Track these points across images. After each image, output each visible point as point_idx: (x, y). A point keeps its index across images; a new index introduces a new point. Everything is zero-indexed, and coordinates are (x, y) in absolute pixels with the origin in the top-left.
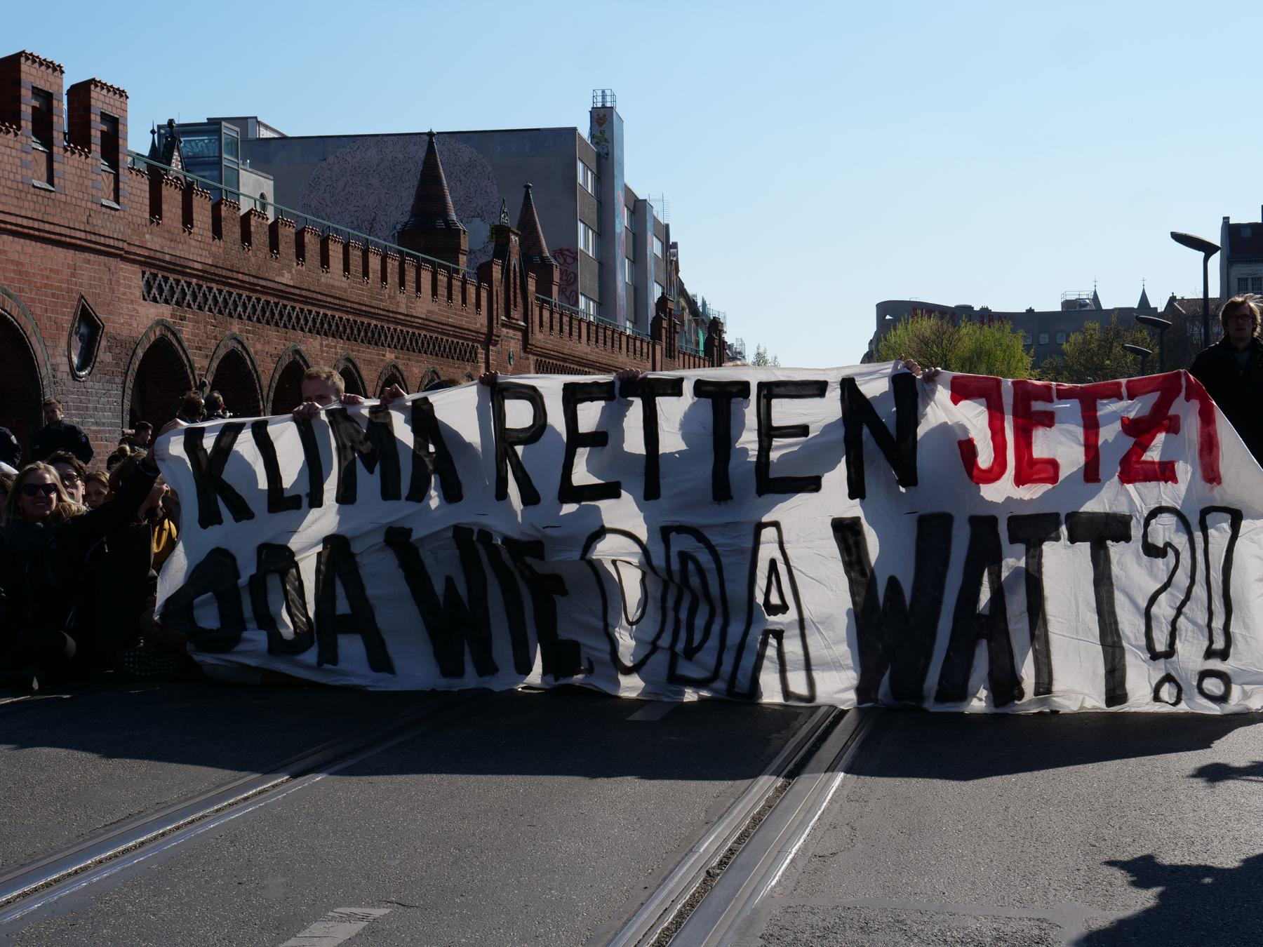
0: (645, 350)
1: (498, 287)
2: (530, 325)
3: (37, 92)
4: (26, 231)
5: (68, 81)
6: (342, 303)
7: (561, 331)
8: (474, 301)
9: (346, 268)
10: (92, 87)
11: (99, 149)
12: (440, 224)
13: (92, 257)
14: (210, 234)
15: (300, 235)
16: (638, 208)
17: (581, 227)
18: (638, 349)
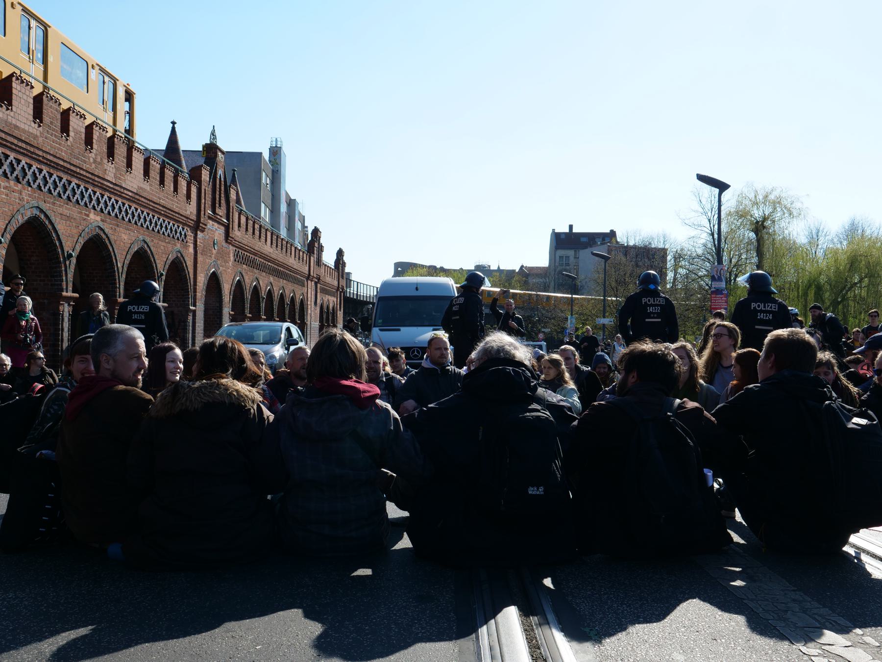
0: (305, 259)
1: (206, 187)
2: (231, 223)
8: (185, 192)
16: (291, 204)
17: (263, 205)
18: (301, 257)
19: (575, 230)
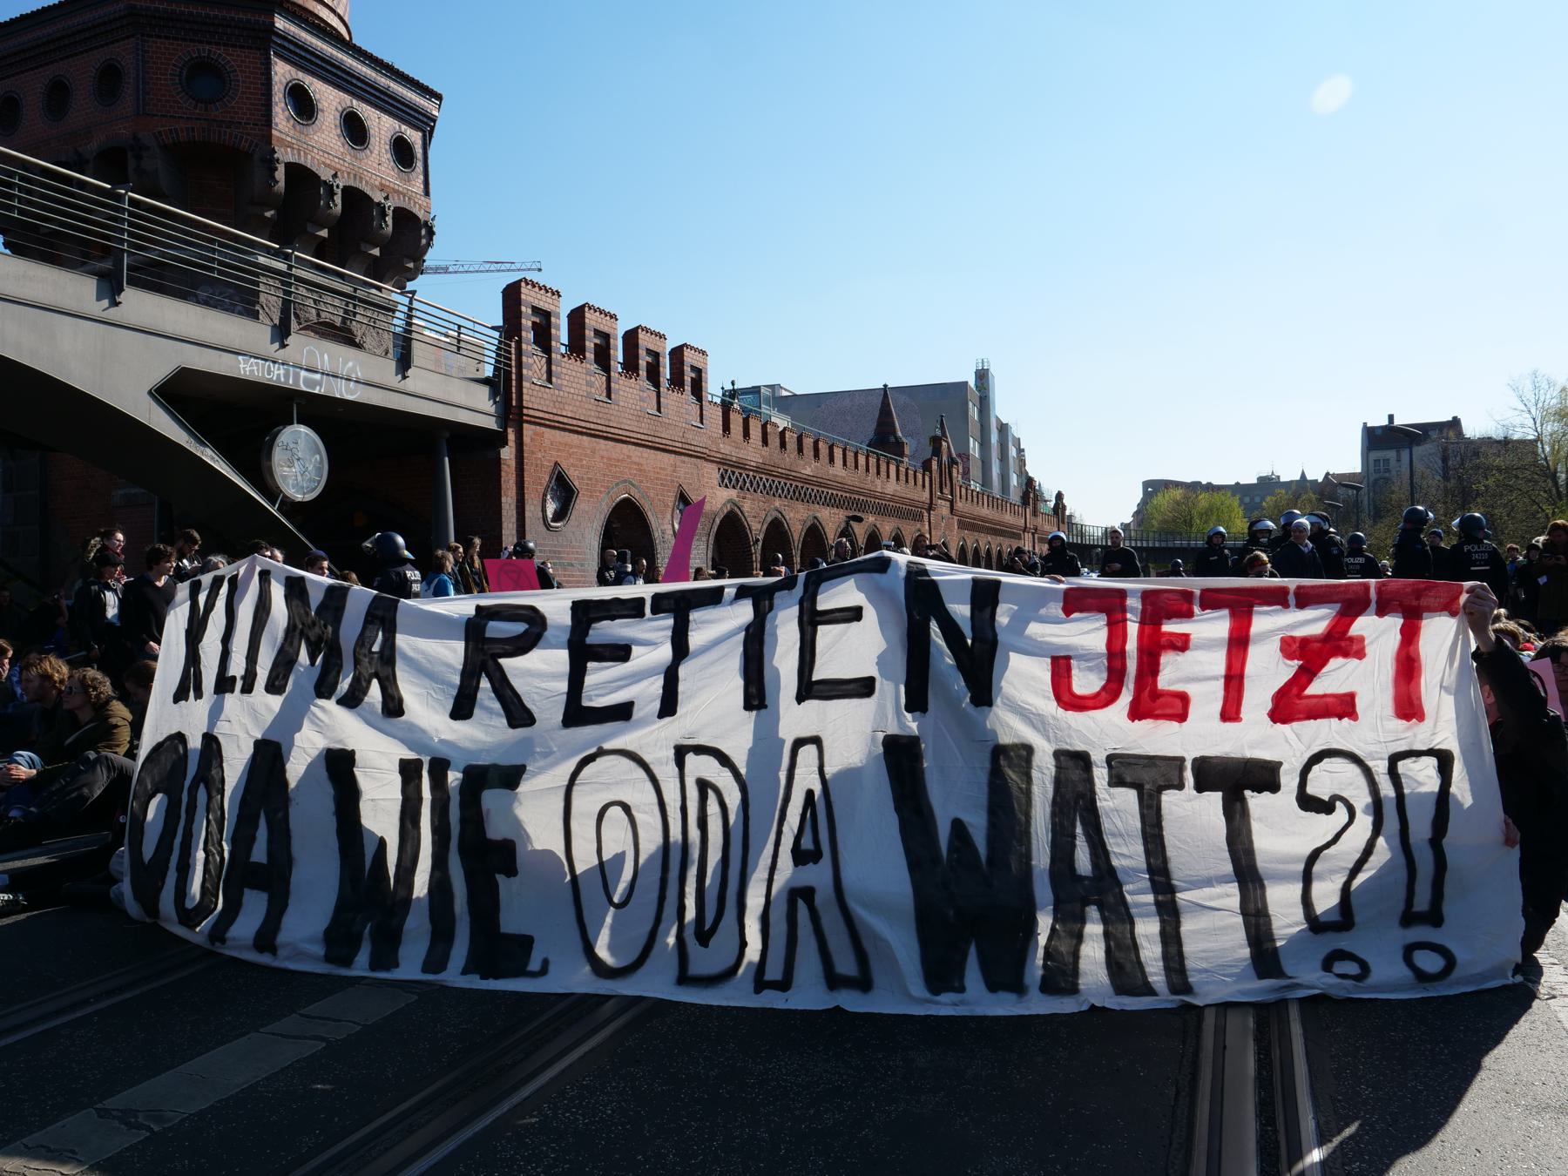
1: (935, 475)
3: (649, 352)
4: (643, 442)
5: (670, 345)
6: (842, 486)
7: (972, 501)
8: (921, 483)
9: (845, 464)
10: (685, 348)
11: (690, 388)
12: (892, 439)
13: (686, 459)
14: (761, 443)
15: (816, 443)
16: (1003, 429)
17: (971, 440)
19: (1397, 422)
